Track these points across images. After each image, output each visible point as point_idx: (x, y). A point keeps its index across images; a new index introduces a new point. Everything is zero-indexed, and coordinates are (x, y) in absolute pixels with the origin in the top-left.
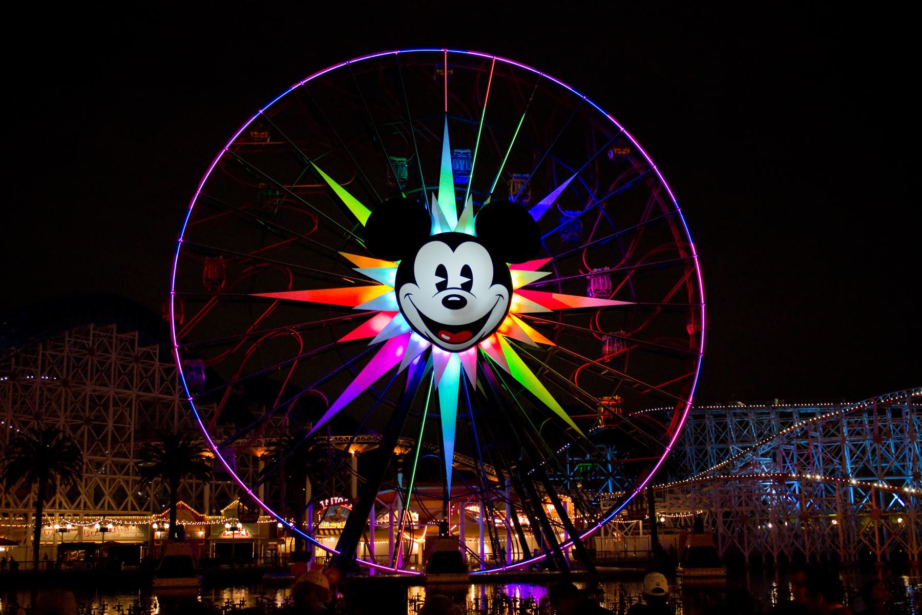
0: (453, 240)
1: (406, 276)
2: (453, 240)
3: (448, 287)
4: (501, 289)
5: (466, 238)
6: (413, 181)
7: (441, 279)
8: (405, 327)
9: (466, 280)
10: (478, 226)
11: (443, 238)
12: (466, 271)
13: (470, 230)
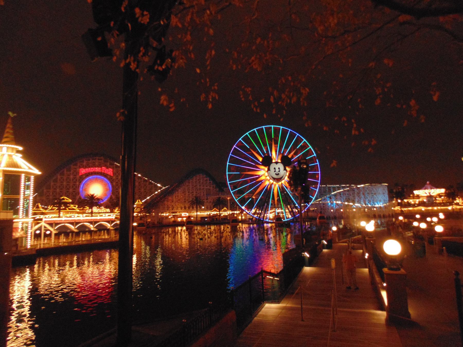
0: (277, 163)
1: (269, 170)
2: (277, 163)
3: (276, 171)
4: (285, 171)
5: (279, 162)
6: (267, 151)
7: (275, 170)
8: (269, 179)
9: (279, 170)
10: (281, 159)
11: (275, 163)
12: (279, 169)
13: (279, 161)
